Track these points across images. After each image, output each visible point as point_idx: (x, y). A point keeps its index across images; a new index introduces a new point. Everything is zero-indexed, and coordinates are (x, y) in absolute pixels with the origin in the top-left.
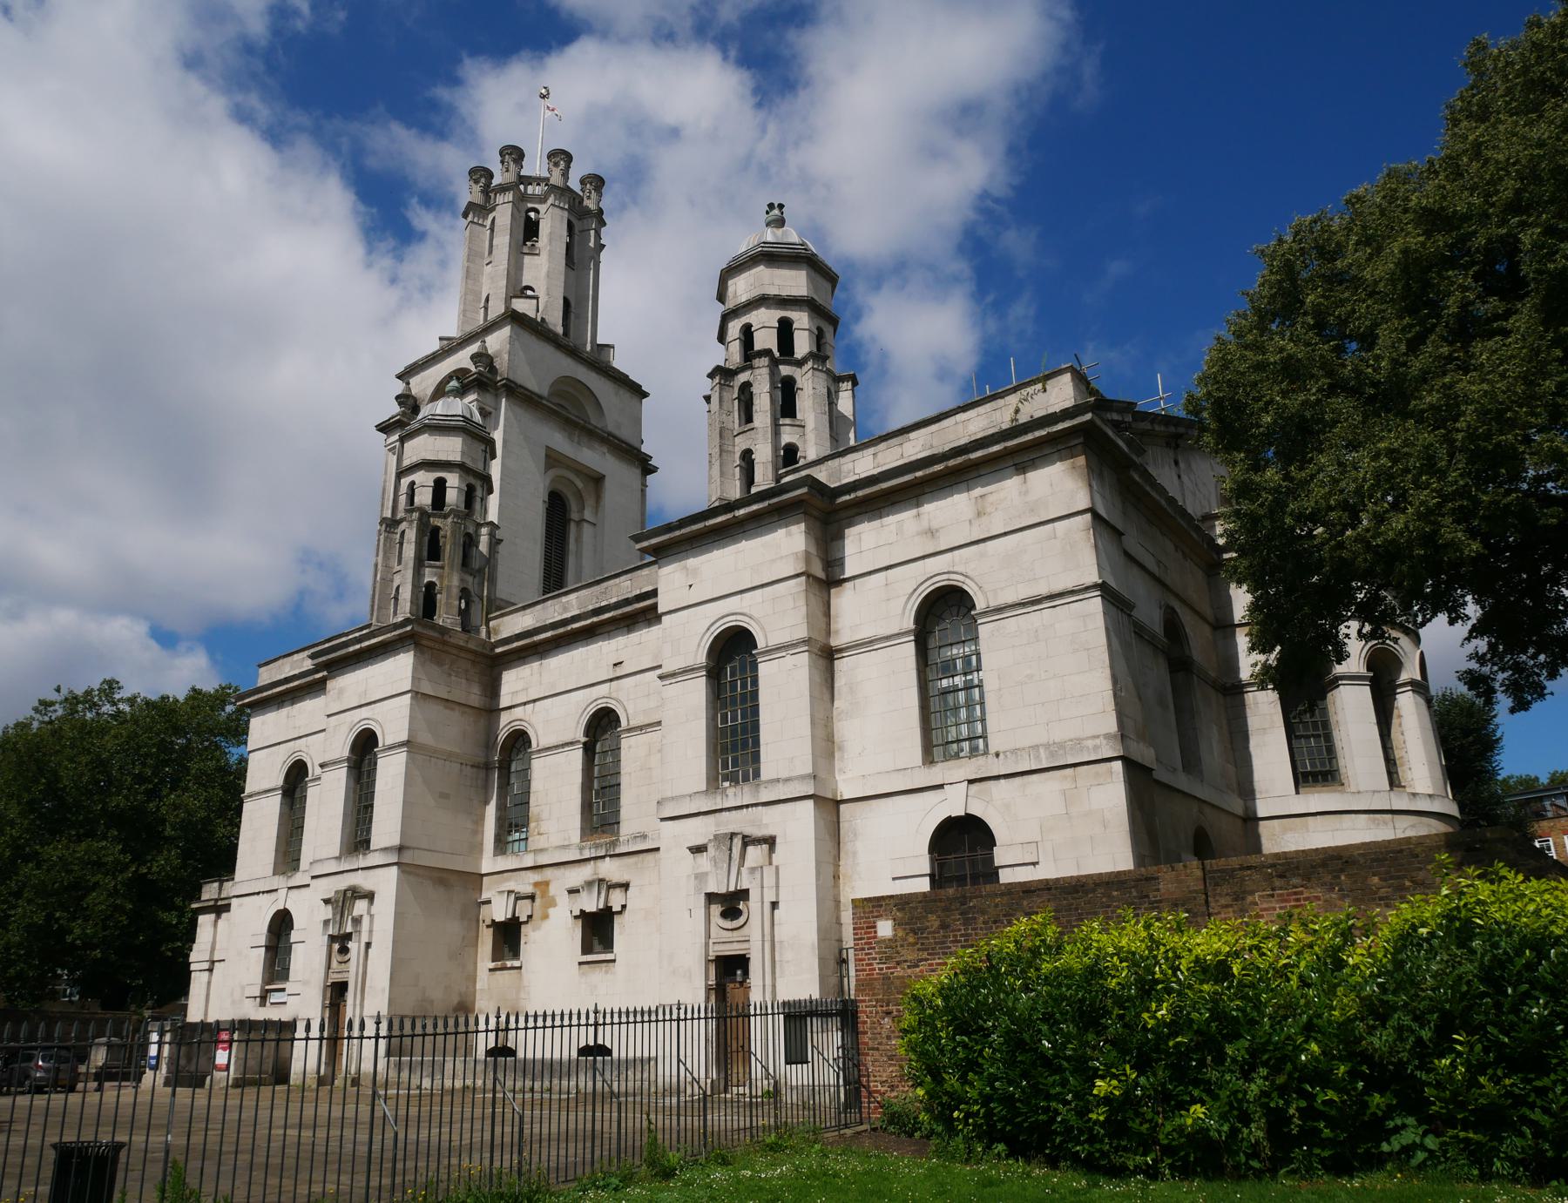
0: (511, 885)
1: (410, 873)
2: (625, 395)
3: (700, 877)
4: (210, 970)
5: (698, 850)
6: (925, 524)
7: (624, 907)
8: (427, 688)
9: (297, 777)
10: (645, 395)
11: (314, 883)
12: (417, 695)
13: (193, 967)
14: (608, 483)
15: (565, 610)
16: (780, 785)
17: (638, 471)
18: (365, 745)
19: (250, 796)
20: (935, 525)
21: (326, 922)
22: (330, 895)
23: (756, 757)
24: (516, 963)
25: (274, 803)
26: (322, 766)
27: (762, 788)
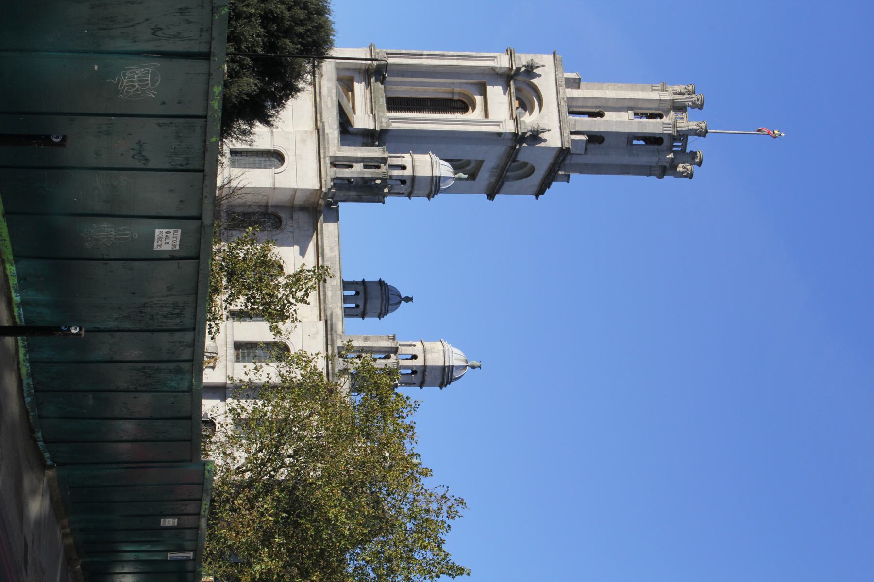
2: (535, 189)
10: (537, 198)
12: (295, 190)
15: (331, 249)
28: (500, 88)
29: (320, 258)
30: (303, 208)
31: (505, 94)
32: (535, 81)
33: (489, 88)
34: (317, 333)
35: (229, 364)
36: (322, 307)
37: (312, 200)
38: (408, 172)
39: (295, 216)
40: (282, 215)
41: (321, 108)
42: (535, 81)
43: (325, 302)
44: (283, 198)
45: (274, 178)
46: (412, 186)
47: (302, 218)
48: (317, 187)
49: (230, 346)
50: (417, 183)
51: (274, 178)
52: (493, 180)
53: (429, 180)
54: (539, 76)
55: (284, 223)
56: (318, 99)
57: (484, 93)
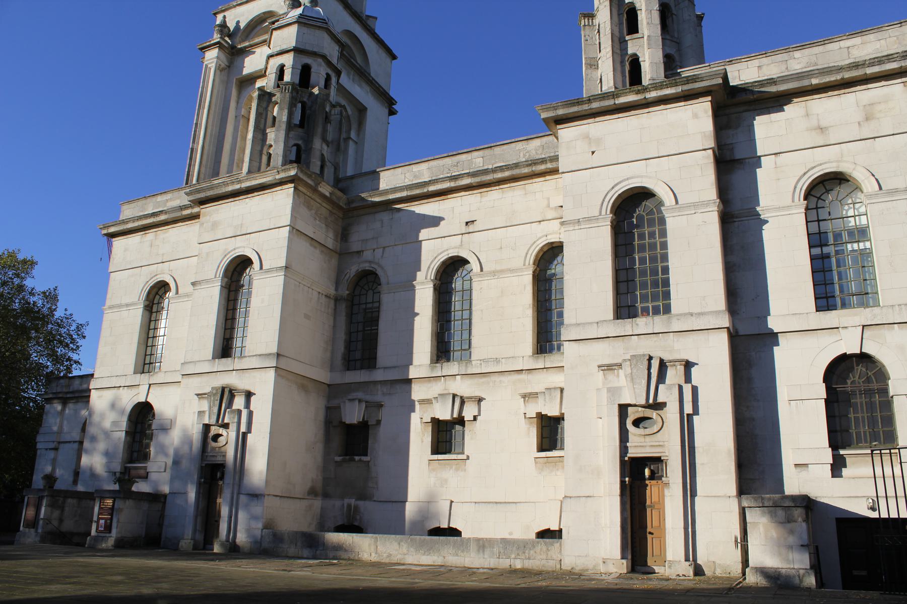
0: (360, 395)
1: (283, 377)
2: (383, 54)
3: (613, 391)
4: (56, 449)
5: (608, 368)
6: (814, 123)
7: (475, 418)
8: (301, 226)
9: (157, 295)
11: (185, 381)
12: (295, 230)
13: (39, 446)
14: (369, 113)
16: (693, 318)
17: (387, 111)
18: (237, 270)
19: (110, 307)
20: (823, 124)
21: (201, 413)
22: (208, 390)
23: (667, 295)
24: (364, 458)
25: (137, 314)
26: (193, 284)
27: (674, 320)
28: (246, 60)
29: (432, 188)
30: (344, 235)
31: (254, 53)
32: (242, 25)
33: (246, 71)
34: (587, 137)
35: (677, 326)
36: (526, 170)
37: (324, 212)
38: (288, 60)
39: (355, 247)
40: (353, 270)
41: (174, 210)
42: (242, 25)
43: (517, 165)
44: (316, 267)
45: (269, 271)
46: (314, 54)
47: (361, 234)
48: (289, 189)
49: (626, 326)
50: (308, 48)
51: (269, 271)
52: (368, 88)
53: (305, 30)
54: (238, 22)
55: (366, 266)
56: (163, 217)
57: (252, 79)
